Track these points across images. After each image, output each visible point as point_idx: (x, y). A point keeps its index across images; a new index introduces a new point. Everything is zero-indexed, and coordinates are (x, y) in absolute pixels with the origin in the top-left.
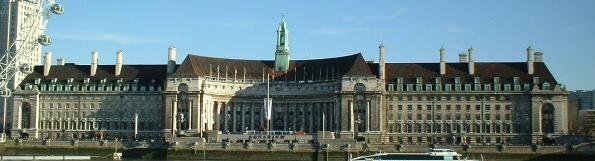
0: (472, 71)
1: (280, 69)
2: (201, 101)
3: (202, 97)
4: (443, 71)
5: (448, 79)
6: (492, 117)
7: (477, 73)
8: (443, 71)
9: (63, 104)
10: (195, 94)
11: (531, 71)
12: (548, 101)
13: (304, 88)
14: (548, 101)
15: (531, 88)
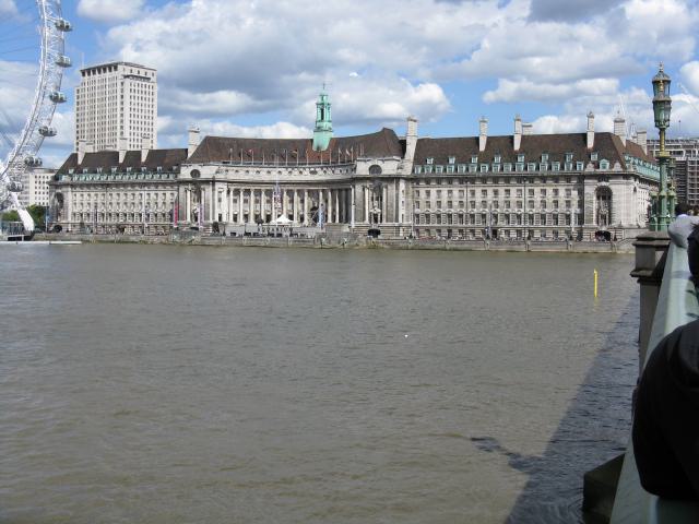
0: (517, 146)
1: (318, 148)
2: (213, 190)
3: (213, 185)
4: (482, 147)
5: (487, 158)
6: (537, 204)
7: (523, 150)
8: (482, 147)
9: (92, 194)
10: (207, 182)
11: (590, 143)
12: (604, 184)
13: (337, 171)
14: (604, 184)
15: (585, 167)
